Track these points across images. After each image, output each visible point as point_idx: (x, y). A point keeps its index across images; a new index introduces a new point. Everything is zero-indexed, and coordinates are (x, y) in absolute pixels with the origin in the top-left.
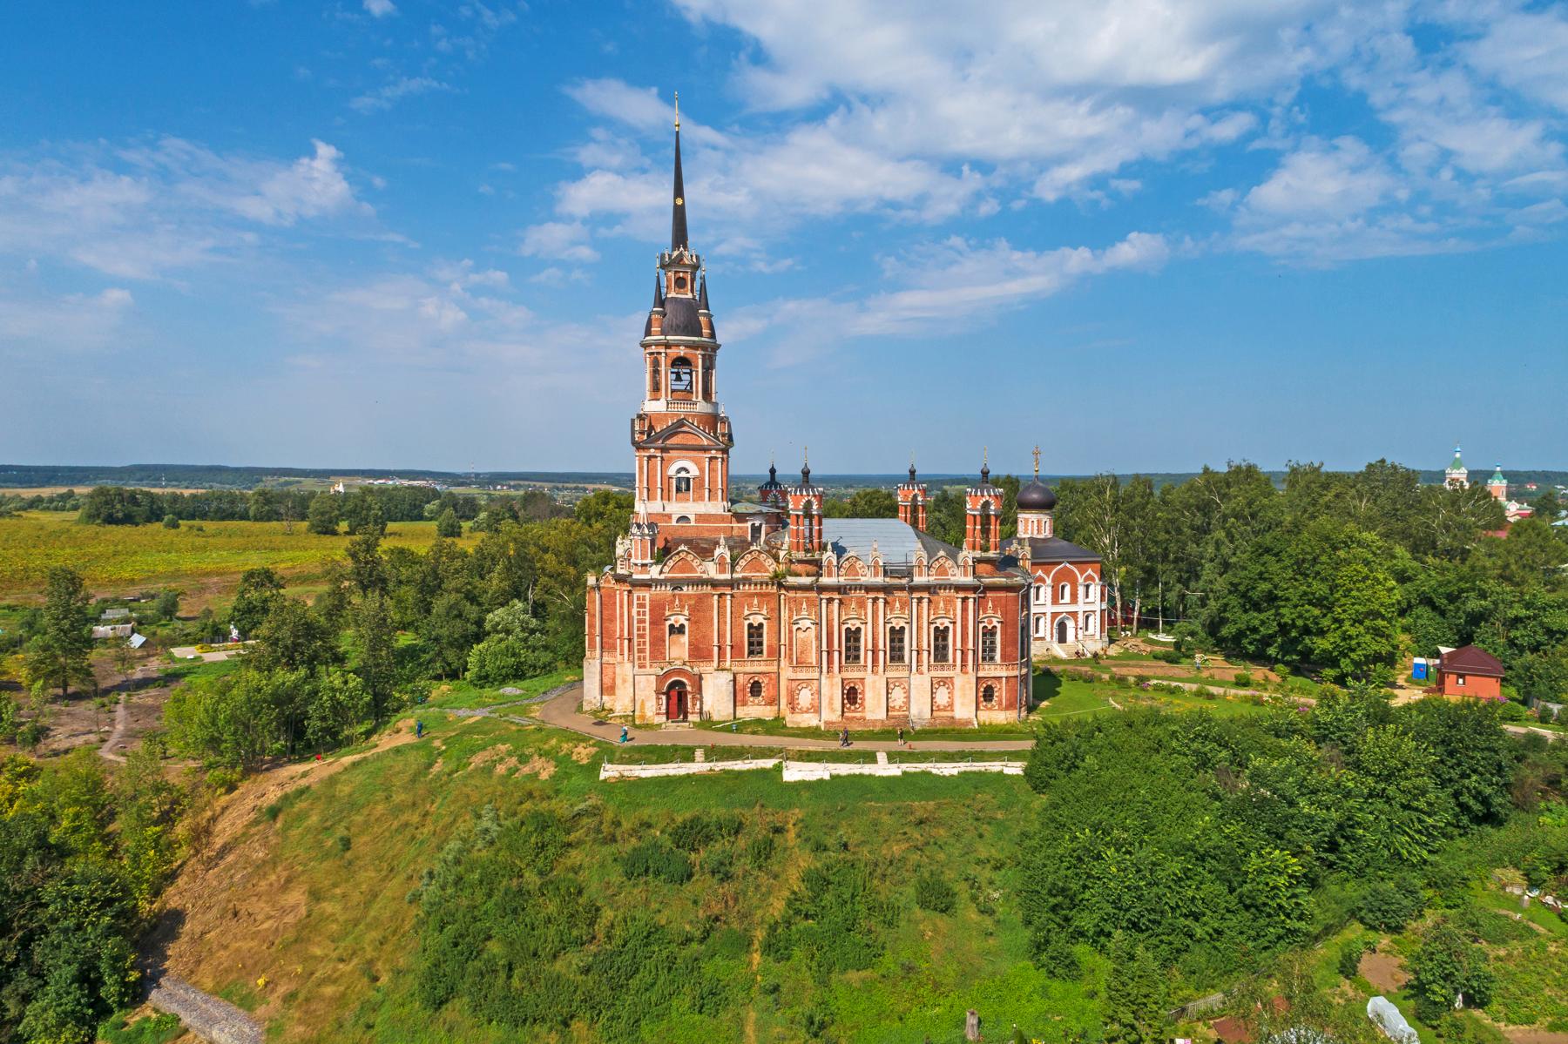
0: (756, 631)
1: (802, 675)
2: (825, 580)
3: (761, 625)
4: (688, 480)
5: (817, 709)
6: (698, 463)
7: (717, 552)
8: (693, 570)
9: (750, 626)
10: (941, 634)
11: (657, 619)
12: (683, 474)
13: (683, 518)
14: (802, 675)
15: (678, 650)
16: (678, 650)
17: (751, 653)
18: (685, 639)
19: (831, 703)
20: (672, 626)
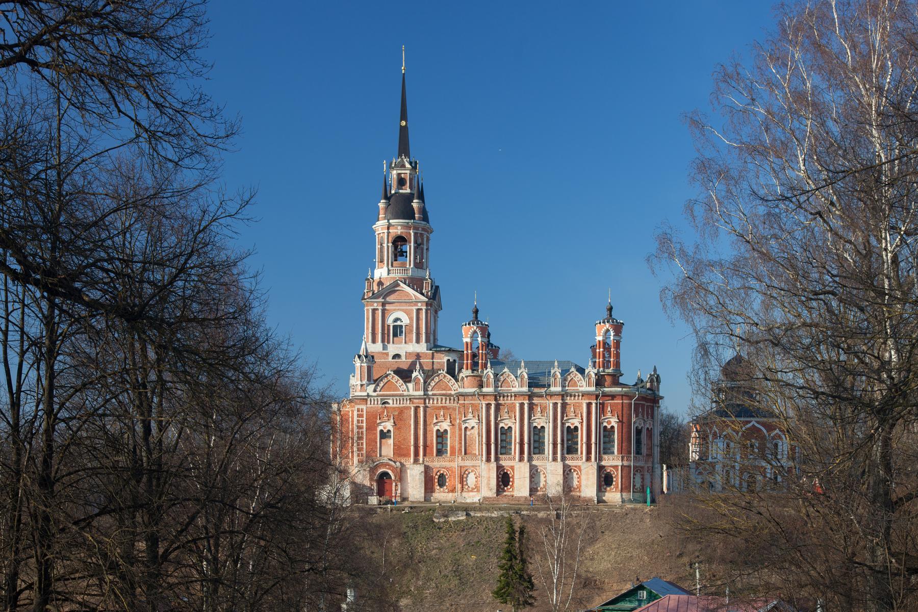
0: (441, 435)
1: (468, 463)
3: (446, 431)
4: (401, 326)
5: (477, 489)
6: (408, 313)
7: (414, 375)
8: (397, 389)
10: (571, 432)
11: (371, 427)
12: (399, 323)
13: (397, 356)
14: (468, 463)
16: (388, 449)
19: (488, 484)
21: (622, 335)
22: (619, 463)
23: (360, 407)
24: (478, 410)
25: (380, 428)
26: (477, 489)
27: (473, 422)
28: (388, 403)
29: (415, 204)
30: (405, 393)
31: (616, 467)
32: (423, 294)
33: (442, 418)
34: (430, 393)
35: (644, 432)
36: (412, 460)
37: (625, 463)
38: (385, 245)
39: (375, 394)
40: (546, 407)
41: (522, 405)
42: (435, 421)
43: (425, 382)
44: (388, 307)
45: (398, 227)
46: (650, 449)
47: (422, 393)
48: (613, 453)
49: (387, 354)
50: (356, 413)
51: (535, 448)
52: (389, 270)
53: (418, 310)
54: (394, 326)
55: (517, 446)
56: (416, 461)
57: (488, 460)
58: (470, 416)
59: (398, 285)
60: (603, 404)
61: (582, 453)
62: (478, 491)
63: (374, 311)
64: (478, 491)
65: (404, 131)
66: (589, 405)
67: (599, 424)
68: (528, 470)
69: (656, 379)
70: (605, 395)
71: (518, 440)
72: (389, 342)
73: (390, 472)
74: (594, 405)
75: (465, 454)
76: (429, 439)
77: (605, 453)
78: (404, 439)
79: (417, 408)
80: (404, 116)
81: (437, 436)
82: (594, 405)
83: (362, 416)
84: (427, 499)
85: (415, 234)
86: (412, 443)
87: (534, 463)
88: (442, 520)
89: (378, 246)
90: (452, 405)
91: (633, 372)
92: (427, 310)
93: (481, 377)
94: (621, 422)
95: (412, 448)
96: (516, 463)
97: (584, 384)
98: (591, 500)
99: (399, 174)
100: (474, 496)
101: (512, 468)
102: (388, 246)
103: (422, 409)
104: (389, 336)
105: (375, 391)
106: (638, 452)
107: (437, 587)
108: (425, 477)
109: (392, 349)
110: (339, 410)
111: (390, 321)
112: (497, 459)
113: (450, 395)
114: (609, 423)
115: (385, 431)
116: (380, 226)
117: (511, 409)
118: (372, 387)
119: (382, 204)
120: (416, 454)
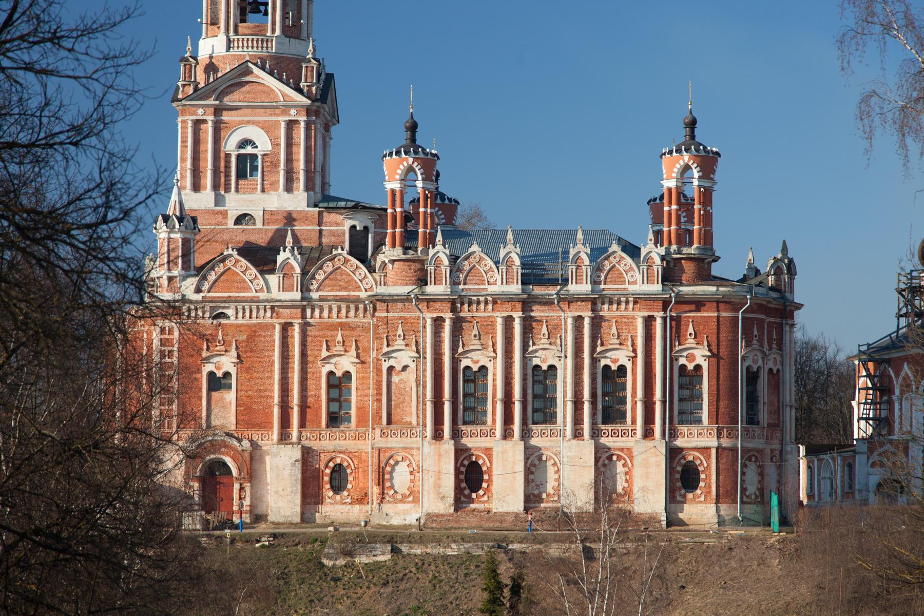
1: (394, 442)
2: (431, 289)
3: (347, 375)
4: (254, 157)
5: (414, 496)
7: (281, 258)
8: (244, 287)
9: (331, 374)
10: (612, 378)
12: (249, 150)
14: (394, 442)
18: (230, 396)
19: (437, 486)
21: (717, 177)
22: (713, 442)
24: (415, 332)
25: (208, 368)
26: (414, 496)
27: (405, 357)
28: (225, 316)
30: (263, 296)
31: (705, 450)
32: (299, 90)
33: (339, 348)
34: (315, 295)
35: (764, 379)
36: (275, 436)
37: (726, 442)
39: (199, 297)
40: (558, 326)
41: (508, 321)
42: (325, 354)
43: (304, 273)
44: (226, 117)
46: (777, 411)
47: (297, 295)
48: (699, 421)
49: (225, 215)
51: (535, 411)
52: (229, 41)
53: (291, 124)
54: (239, 156)
55: (499, 407)
56: (284, 438)
57: (438, 435)
58: (399, 343)
59: (249, 72)
60: (677, 320)
61: (634, 422)
62: (416, 501)
63: (198, 124)
64: (416, 501)
66: (649, 321)
67: (670, 360)
68: (520, 457)
69: (786, 268)
70: (682, 301)
71: (500, 394)
72: (227, 190)
73: (228, 460)
74: (659, 323)
75: (389, 422)
76: (311, 391)
77: (682, 422)
78: (260, 392)
79: (286, 328)
81: (330, 386)
82: (659, 323)
84: (306, 517)
86: (276, 399)
87: (534, 441)
88: (341, 562)
90: (361, 320)
91: (740, 252)
92: (308, 124)
93: (422, 262)
94: (715, 356)
95: (276, 411)
97: (639, 277)
98: (653, 519)
100: (406, 512)
101: (488, 452)
103: (297, 329)
104: (228, 176)
105: (198, 290)
106: (752, 419)
108: (303, 473)
109: (235, 203)
111: (230, 145)
112: (456, 434)
113: (357, 300)
114: (691, 358)
115: (219, 374)
117: (487, 327)
118: (192, 282)
120: (285, 423)
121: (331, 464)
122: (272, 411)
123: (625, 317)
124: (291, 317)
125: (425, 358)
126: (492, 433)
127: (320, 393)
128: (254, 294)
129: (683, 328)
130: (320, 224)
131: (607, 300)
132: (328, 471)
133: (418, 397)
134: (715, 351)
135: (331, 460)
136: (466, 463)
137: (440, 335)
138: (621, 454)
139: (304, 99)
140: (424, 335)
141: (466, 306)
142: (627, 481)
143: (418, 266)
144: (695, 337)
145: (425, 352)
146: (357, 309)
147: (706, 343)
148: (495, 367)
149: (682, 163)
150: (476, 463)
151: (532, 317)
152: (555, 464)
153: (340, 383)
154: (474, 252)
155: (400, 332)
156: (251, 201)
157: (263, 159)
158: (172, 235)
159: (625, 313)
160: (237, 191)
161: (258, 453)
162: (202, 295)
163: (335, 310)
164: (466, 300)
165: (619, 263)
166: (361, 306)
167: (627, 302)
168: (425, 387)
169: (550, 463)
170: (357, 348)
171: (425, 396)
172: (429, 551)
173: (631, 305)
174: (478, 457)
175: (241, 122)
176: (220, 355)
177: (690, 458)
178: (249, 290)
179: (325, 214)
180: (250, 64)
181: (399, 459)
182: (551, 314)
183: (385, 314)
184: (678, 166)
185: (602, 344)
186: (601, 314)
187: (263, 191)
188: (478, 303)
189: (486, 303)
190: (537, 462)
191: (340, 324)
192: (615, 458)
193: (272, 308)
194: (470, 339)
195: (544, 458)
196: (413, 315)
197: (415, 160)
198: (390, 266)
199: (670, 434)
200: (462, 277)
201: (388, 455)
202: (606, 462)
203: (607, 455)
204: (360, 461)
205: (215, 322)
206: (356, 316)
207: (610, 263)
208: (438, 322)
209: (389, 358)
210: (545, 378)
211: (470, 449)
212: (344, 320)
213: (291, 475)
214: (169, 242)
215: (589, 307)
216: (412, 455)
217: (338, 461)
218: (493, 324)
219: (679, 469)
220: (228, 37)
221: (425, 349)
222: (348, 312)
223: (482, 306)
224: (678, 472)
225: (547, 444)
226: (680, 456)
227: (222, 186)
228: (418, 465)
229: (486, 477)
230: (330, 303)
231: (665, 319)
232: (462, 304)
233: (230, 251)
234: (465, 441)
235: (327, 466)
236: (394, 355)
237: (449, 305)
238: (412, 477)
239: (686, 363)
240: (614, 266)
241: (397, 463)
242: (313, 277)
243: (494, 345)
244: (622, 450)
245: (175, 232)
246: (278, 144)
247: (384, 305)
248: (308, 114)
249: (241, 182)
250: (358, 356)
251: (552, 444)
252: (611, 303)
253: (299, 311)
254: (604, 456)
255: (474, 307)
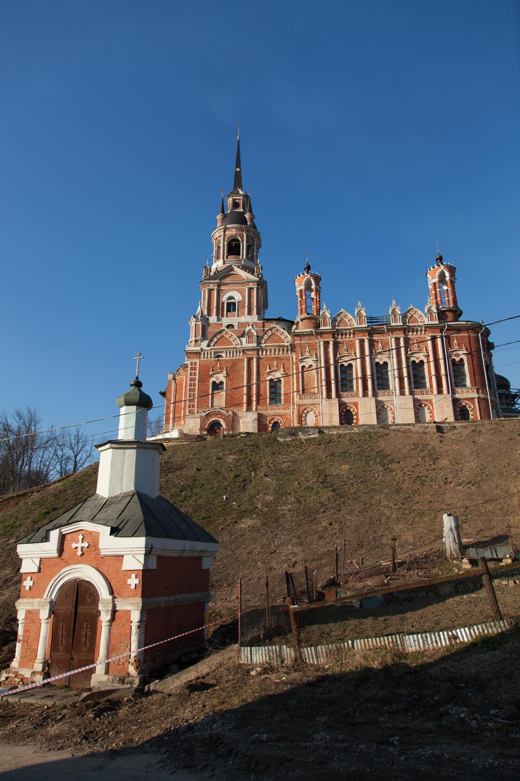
1: (306, 401)
4: (234, 304)
11: (204, 378)
12: (232, 301)
14: (306, 401)
15: (220, 400)
16: (220, 400)
17: (271, 399)
20: (214, 383)
22: (476, 395)
23: (194, 361)
24: (315, 349)
25: (213, 379)
28: (220, 356)
29: (247, 216)
31: (472, 399)
34: (263, 345)
37: (482, 396)
38: (221, 245)
41: (362, 342)
42: (268, 370)
44: (222, 288)
45: (233, 231)
47: (255, 345)
48: (465, 386)
49: (221, 325)
50: (189, 377)
51: (378, 385)
53: (250, 290)
54: (228, 304)
56: (249, 409)
57: (329, 396)
59: (232, 270)
60: (448, 338)
61: (431, 387)
63: (210, 291)
65: (238, 177)
67: (447, 356)
68: (374, 405)
70: (451, 329)
71: (360, 375)
72: (223, 316)
74: (439, 341)
76: (262, 388)
77: (457, 386)
79: (250, 360)
80: (238, 165)
81: (271, 387)
82: (439, 341)
83: (195, 369)
85: (248, 236)
87: (379, 398)
88: (289, 439)
89: (215, 248)
90: (285, 355)
94: (469, 354)
95: (245, 397)
96: (361, 400)
99: (234, 200)
101: (356, 404)
102: (223, 245)
103: (255, 360)
104: (223, 311)
105: (208, 345)
107: (299, 502)
110: (174, 379)
111: (224, 298)
112: (338, 396)
115: (218, 382)
116: (218, 234)
117: (351, 345)
118: (206, 342)
119: (219, 217)
121: (272, 422)
122: (243, 398)
123: (420, 338)
124: (252, 355)
125: (320, 361)
126: (357, 395)
127: (266, 389)
128: (235, 346)
129: (451, 341)
130: (263, 327)
131: (411, 330)
132: (271, 425)
133: (318, 380)
134: (470, 351)
135: (272, 419)
136: (344, 410)
137: (327, 350)
138: (426, 403)
139: (256, 278)
140: (320, 350)
141: (340, 336)
142: (431, 417)
143: (314, 321)
144: (458, 346)
145: (320, 358)
146: (283, 350)
147: (464, 348)
148: (356, 364)
149: (440, 270)
150: (349, 411)
151: (373, 340)
152: (391, 410)
153: (276, 385)
154: (342, 312)
155: (307, 349)
156: (233, 320)
157: (238, 304)
158: (197, 323)
159: (421, 336)
160: (227, 316)
161: (236, 418)
162: (210, 347)
163: (273, 351)
164: (340, 332)
165: (415, 314)
166: (285, 348)
167: (421, 331)
168: (321, 375)
169: (388, 409)
170: (284, 368)
171: (321, 378)
172: (341, 432)
173: (423, 332)
174: (350, 407)
175: (228, 290)
176: (218, 373)
177: (464, 404)
178: (233, 345)
179: (266, 324)
180: (233, 266)
181: (309, 410)
182: (383, 338)
183: (300, 342)
184: (438, 272)
185: (410, 351)
186: (408, 337)
187: (238, 316)
188: (346, 335)
189: (350, 335)
190: (382, 409)
191: (276, 357)
192: (423, 405)
193: (243, 351)
194: (343, 350)
195: (385, 407)
196: (313, 341)
197: (311, 276)
198: (301, 323)
199: (452, 392)
200: (337, 324)
201: (303, 408)
202: (419, 408)
203: (419, 404)
204: (287, 419)
205: (216, 359)
206: (283, 354)
207: (410, 314)
208: (326, 344)
209: (302, 362)
210: (382, 369)
211: (346, 404)
212: (277, 356)
213: (252, 426)
214: (196, 326)
215: (402, 333)
216: (316, 408)
217: (276, 420)
218: (354, 344)
219: (458, 409)
220: (224, 260)
221: (320, 356)
222: (279, 352)
223: (348, 336)
224: (458, 411)
225: (387, 399)
226: (458, 403)
227: (220, 314)
228: (319, 413)
229: (355, 417)
230: (271, 347)
231: (442, 337)
232: (338, 335)
233: (224, 328)
234: (343, 399)
235: (270, 423)
236: (305, 360)
237: (332, 335)
238: (317, 419)
239: (455, 357)
240: (412, 315)
241: (308, 412)
242: (262, 338)
243: (355, 354)
244: (426, 401)
245: (199, 322)
246: (245, 297)
247: (299, 338)
248: (258, 285)
249: (228, 313)
250: (284, 371)
251: (390, 399)
252: (413, 332)
253: (256, 352)
254: (417, 404)
255: (344, 336)
